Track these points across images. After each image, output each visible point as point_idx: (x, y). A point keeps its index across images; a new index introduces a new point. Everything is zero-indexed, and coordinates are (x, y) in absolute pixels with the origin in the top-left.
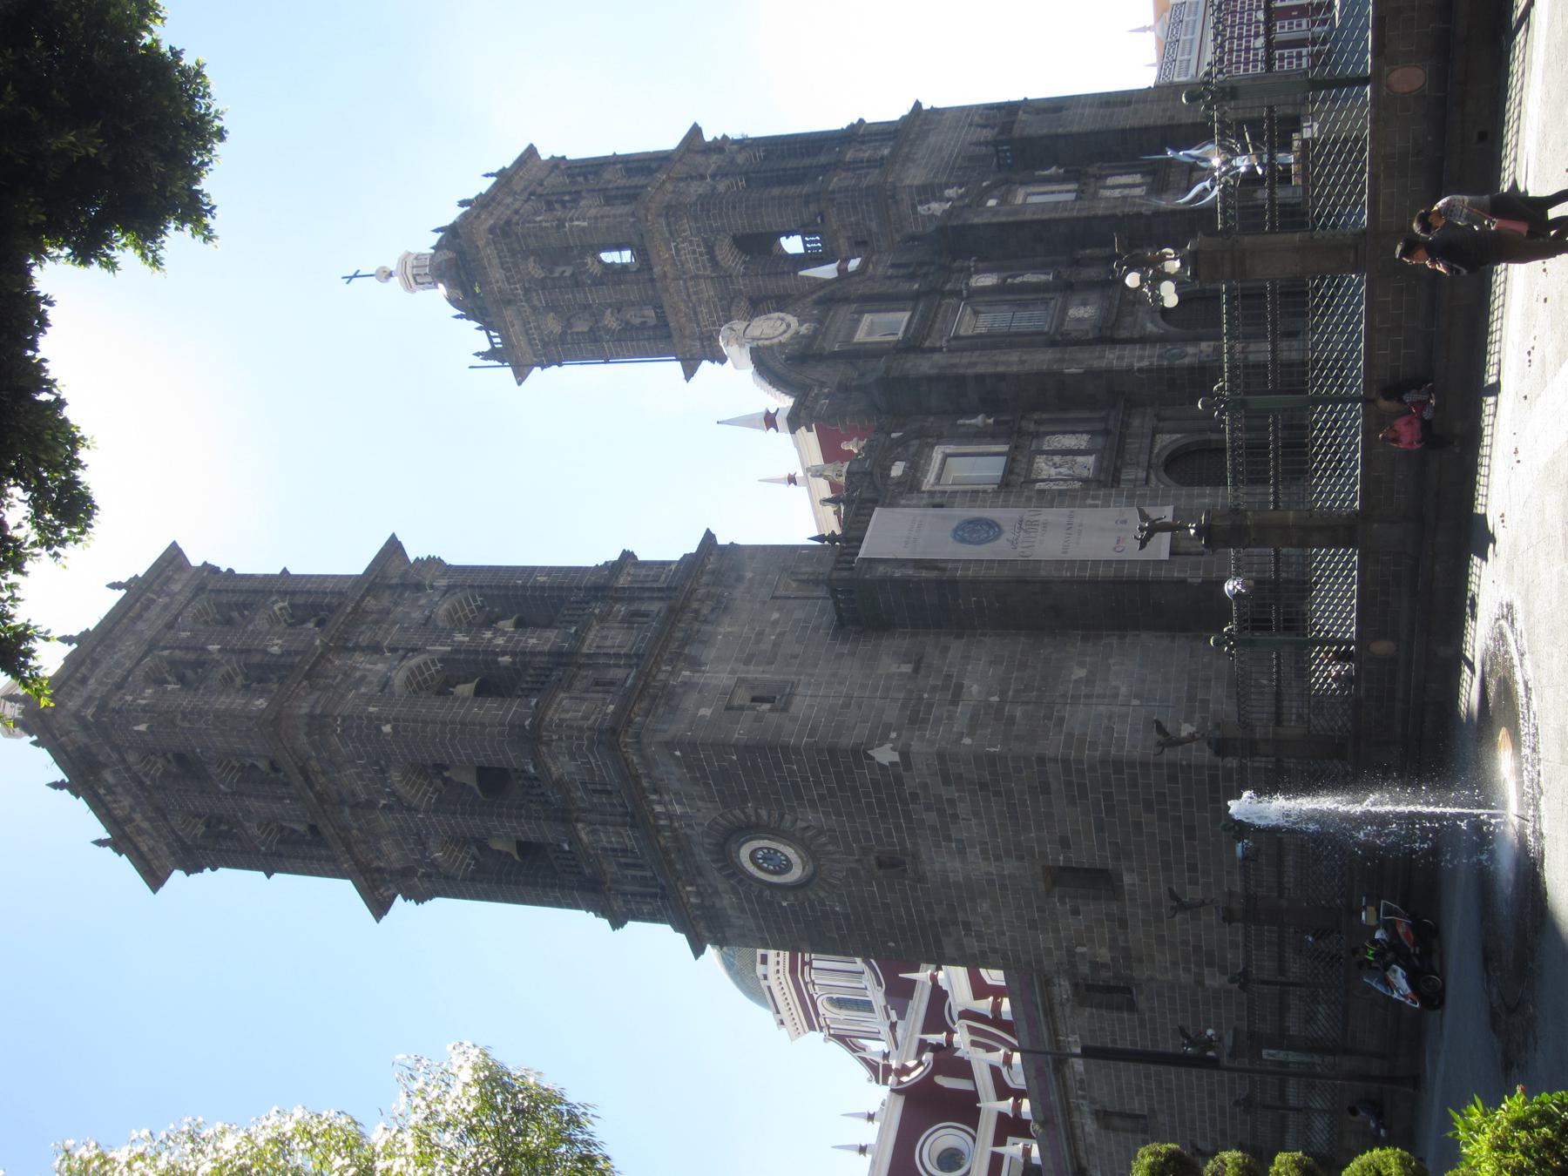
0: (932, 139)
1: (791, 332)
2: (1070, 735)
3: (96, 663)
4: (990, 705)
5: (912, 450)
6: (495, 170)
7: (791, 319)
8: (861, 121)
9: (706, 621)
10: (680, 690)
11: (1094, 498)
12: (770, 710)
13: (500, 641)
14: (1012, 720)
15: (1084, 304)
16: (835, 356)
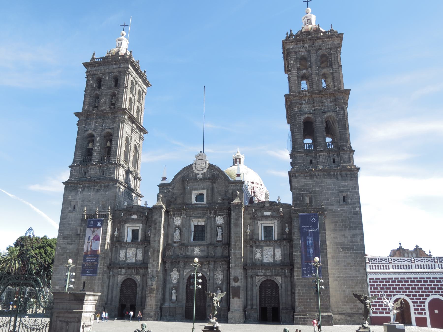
0: (328, 182)
1: (198, 172)
2: (58, 266)
3: (99, 65)
4: (67, 250)
5: (141, 218)
6: (333, 28)
7: (205, 170)
8: (353, 151)
9: (94, 189)
10: (76, 191)
11: (100, 265)
12: (70, 210)
13: (96, 148)
14: (63, 255)
15: (201, 251)
16: (184, 188)
